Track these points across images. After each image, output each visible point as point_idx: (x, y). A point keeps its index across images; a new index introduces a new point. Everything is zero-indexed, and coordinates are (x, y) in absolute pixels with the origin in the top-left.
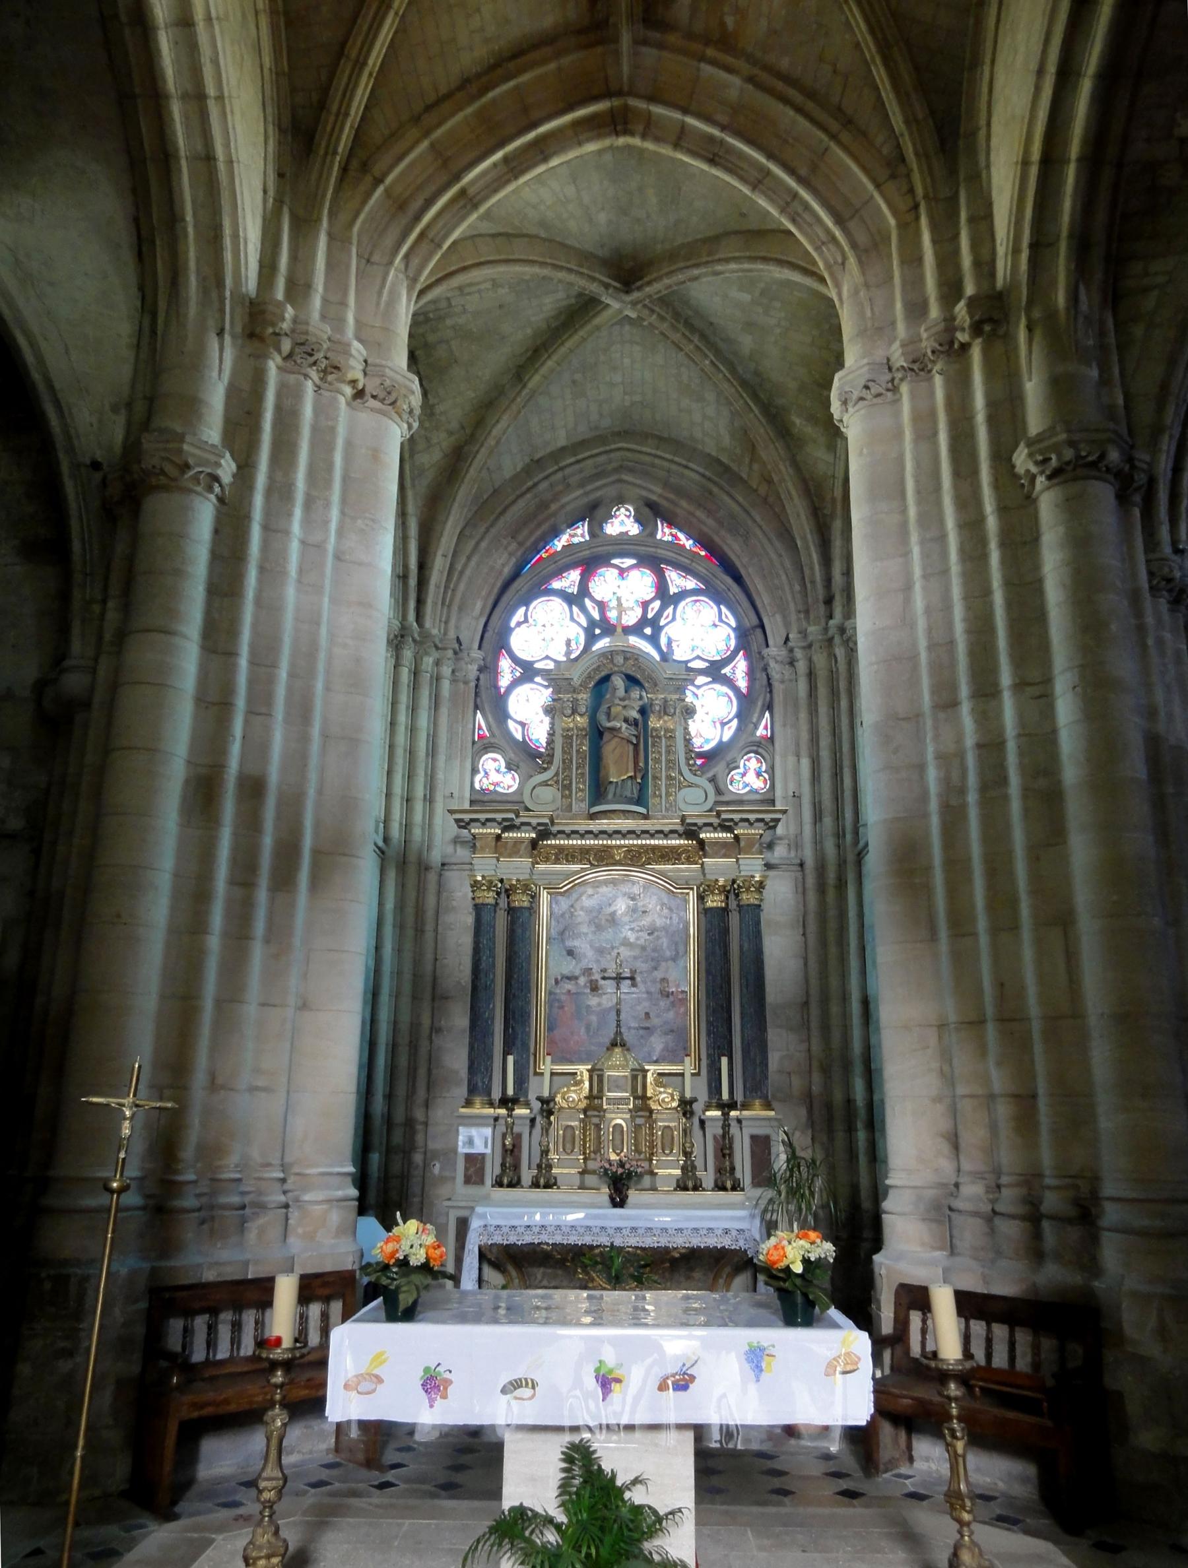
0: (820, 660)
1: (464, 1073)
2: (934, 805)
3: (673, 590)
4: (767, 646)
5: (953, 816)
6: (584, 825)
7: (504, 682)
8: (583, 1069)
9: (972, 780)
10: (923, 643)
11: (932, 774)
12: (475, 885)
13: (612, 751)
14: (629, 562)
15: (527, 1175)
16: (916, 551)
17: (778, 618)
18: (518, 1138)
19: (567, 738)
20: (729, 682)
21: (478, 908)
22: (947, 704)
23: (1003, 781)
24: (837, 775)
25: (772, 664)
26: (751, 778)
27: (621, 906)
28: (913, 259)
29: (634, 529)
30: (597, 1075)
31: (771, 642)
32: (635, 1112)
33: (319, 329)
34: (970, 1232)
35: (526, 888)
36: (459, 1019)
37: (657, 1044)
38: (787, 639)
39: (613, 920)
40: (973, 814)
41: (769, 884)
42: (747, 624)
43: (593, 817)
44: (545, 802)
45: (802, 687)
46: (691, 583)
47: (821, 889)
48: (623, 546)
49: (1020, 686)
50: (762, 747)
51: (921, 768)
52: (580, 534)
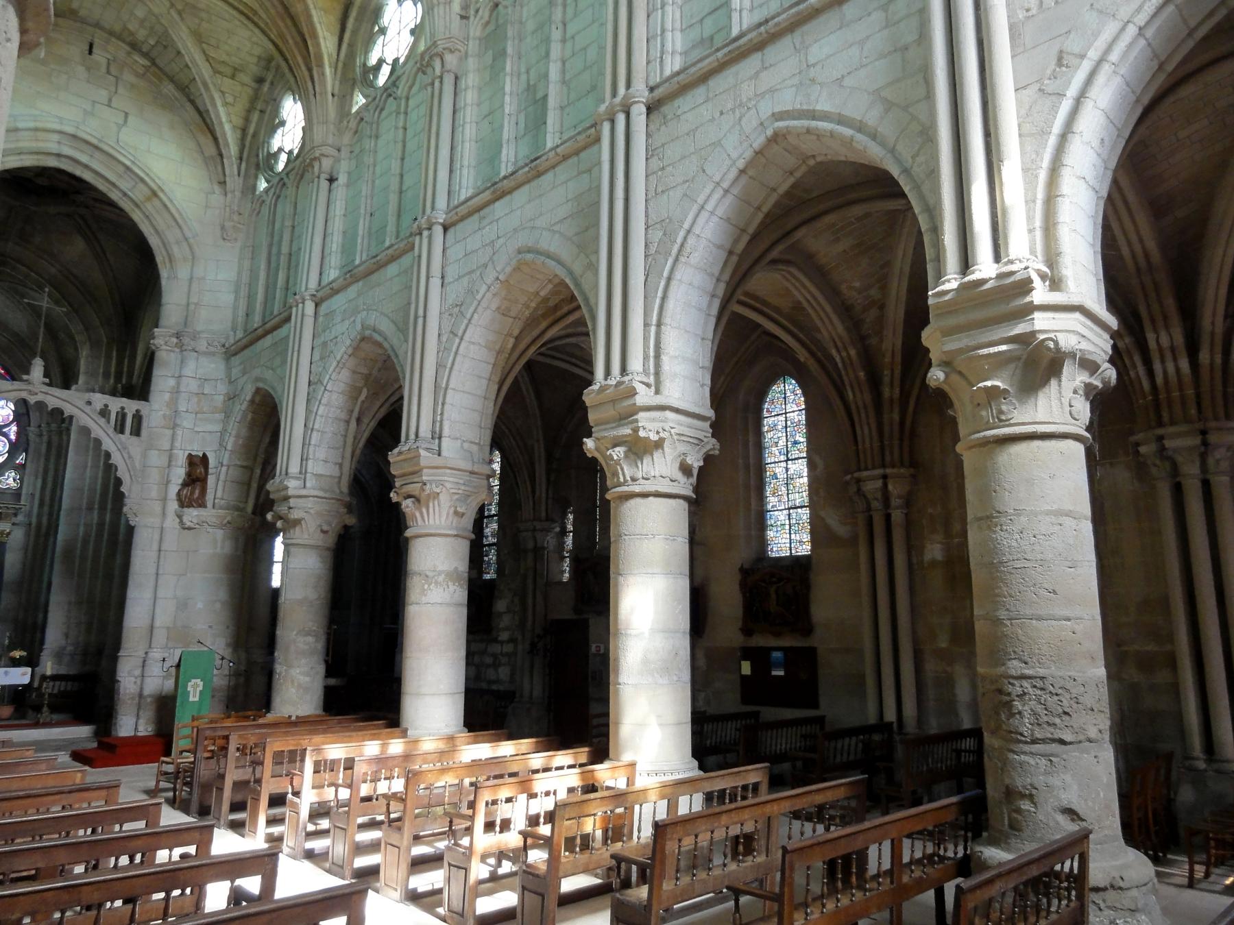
0: (55, 439)
2: (80, 539)
4: (29, 426)
5: (85, 542)
9: (93, 534)
10: (86, 488)
11: (82, 529)
16: (90, 458)
17: (38, 414)
20: (6, 435)
22: (90, 508)
23: (103, 536)
24: (51, 506)
25: (30, 434)
26: (11, 481)
28: (108, 357)
31: (32, 424)
34: (66, 659)
38: (40, 426)
40: (92, 543)
41: (13, 533)
42: (21, 411)
45: (44, 448)
47: (38, 535)
49: (112, 510)
50: (21, 468)
51: (78, 525)
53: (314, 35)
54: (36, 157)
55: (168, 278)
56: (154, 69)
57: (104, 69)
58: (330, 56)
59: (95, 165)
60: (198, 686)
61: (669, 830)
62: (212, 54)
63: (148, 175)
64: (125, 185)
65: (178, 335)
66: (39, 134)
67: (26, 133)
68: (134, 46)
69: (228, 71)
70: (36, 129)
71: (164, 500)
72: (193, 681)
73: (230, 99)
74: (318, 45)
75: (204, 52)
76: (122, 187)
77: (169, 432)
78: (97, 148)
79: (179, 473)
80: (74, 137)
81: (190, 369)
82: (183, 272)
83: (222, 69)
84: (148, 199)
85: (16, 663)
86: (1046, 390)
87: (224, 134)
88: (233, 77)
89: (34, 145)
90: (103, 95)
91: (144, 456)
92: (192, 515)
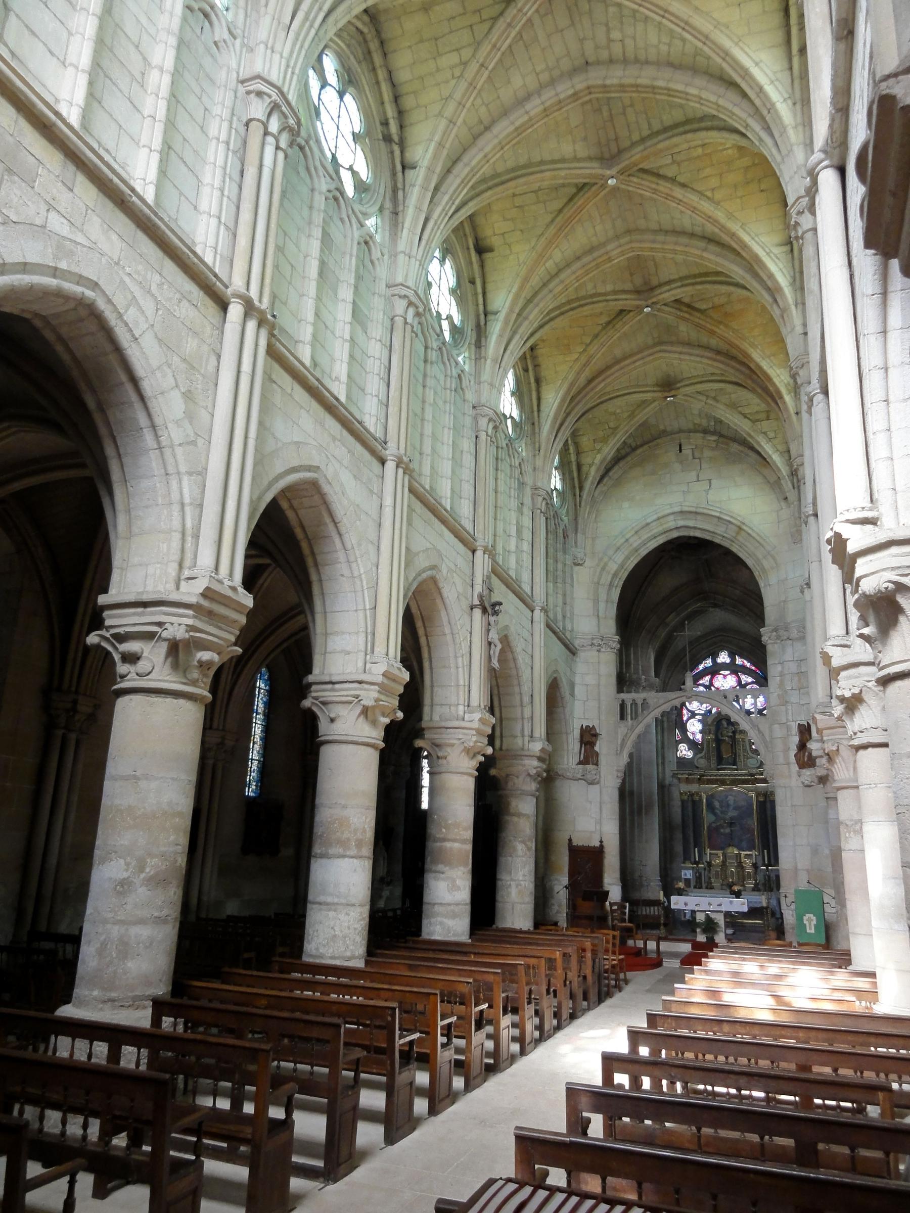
1: (682, 852)
3: (743, 683)
6: (715, 772)
7: (685, 718)
8: (720, 853)
12: (681, 794)
13: (723, 748)
14: (727, 672)
15: (704, 885)
18: (700, 874)
19: (708, 742)
21: (683, 802)
27: (731, 799)
29: (728, 660)
30: (724, 855)
32: (737, 867)
33: (634, 677)
35: (697, 794)
36: (679, 836)
37: (744, 844)
39: (728, 805)
43: (719, 769)
44: (702, 762)
46: (750, 680)
48: (724, 666)
52: (708, 663)
53: (769, 379)
54: (664, 536)
55: (765, 586)
56: (721, 439)
57: (691, 457)
58: (787, 385)
59: (699, 525)
60: (812, 920)
61: (658, 1019)
62: (747, 411)
63: (732, 517)
64: (720, 530)
65: (776, 630)
66: (661, 520)
67: (654, 524)
68: (705, 431)
69: (763, 416)
70: (659, 519)
71: (788, 764)
72: (808, 916)
73: (771, 435)
74: (774, 384)
75: (741, 413)
76: (719, 532)
77: (783, 708)
78: (696, 513)
79: (796, 739)
80: (681, 512)
81: (788, 656)
82: (773, 579)
83: (757, 417)
84: (738, 533)
85: (738, 895)
86: (899, 628)
87: (774, 462)
88: (768, 419)
89: (660, 529)
90: (694, 474)
91: (771, 731)
92: (807, 772)
